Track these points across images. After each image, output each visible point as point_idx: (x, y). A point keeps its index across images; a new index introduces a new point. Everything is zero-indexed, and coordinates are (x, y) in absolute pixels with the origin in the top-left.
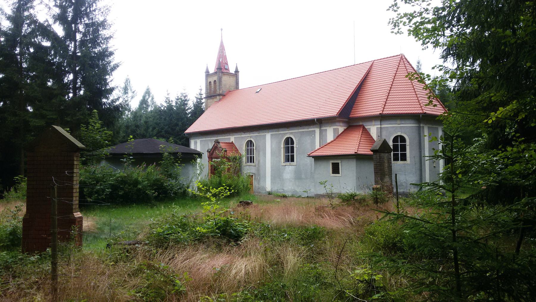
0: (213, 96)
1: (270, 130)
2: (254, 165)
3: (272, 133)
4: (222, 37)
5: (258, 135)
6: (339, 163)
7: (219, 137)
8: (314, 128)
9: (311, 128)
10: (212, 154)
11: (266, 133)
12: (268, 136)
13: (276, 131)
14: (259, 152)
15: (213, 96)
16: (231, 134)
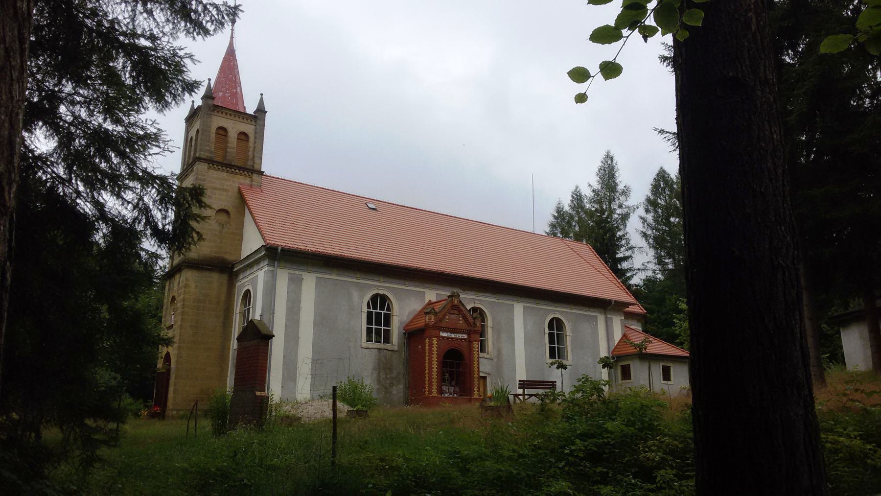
0: (240, 168)
1: (522, 299)
2: (488, 356)
3: (525, 305)
4: (232, 37)
5: (497, 301)
6: (670, 367)
7: (391, 283)
8: (594, 312)
9: (591, 311)
10: (441, 320)
11: (513, 301)
12: (519, 309)
13: (533, 303)
14: (497, 331)
15: (240, 168)
16: (426, 285)
